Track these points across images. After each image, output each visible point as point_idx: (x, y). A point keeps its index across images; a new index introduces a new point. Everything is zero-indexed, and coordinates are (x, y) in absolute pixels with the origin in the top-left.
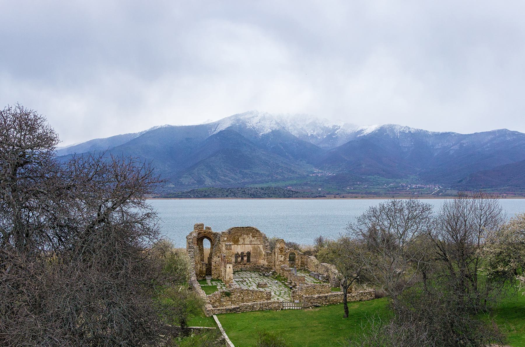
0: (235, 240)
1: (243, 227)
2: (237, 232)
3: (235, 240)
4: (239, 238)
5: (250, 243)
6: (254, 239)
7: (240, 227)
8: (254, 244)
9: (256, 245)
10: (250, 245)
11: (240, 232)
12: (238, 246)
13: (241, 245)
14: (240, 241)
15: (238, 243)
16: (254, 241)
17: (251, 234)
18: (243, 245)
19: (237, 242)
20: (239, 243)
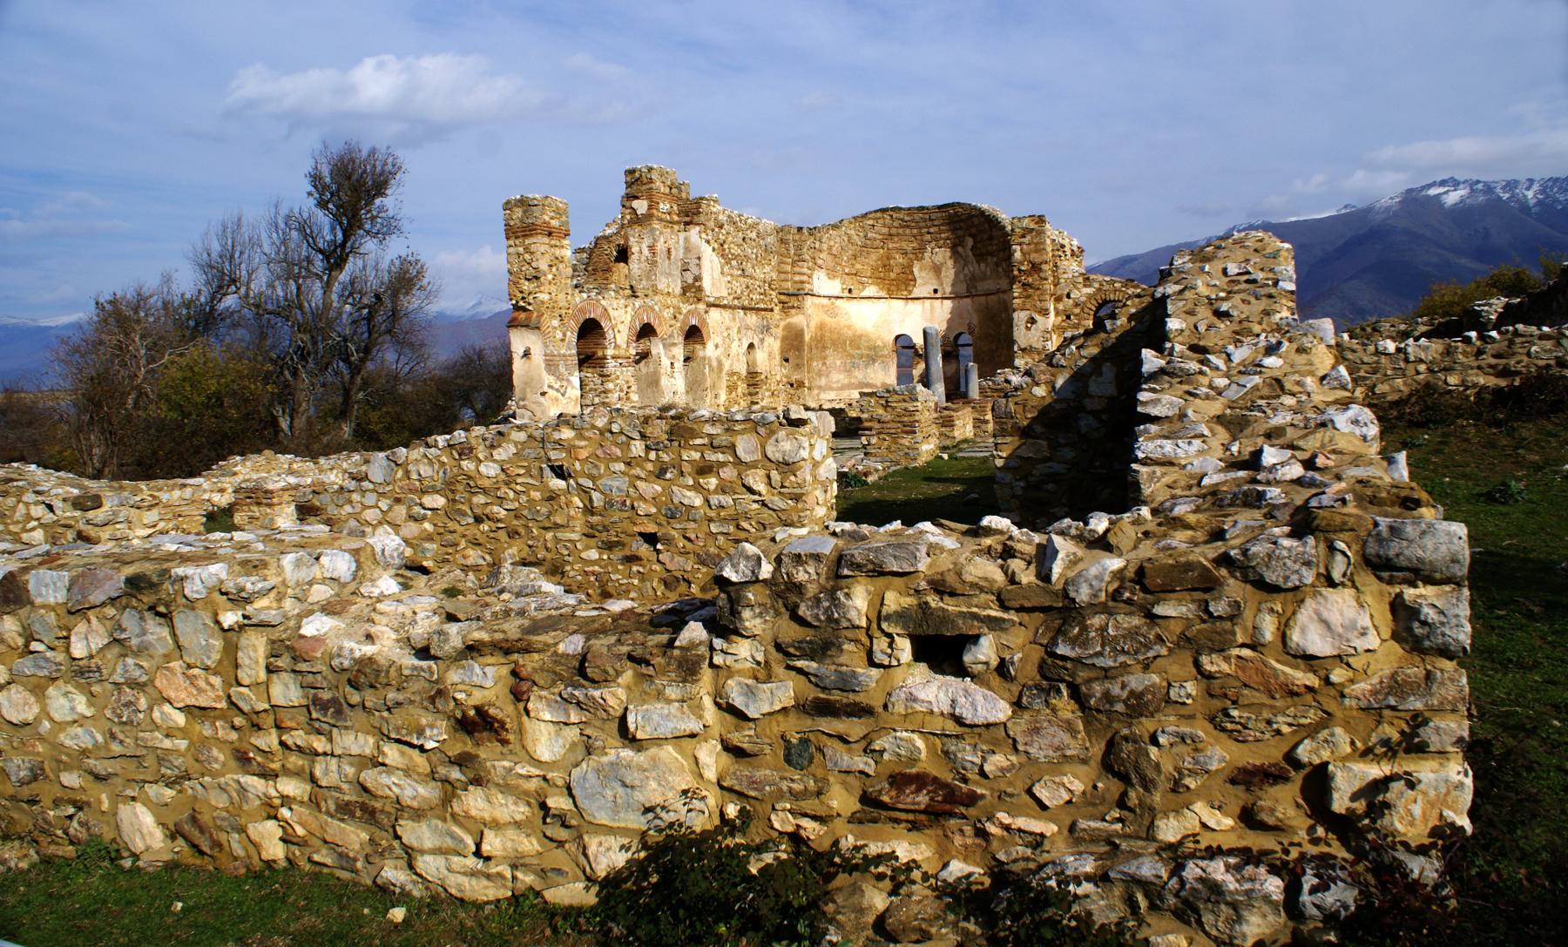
0: (893, 275)
1: (921, 209)
2: (894, 231)
3: (893, 275)
4: (910, 266)
5: (968, 291)
6: (983, 265)
7: (909, 209)
8: (987, 295)
9: (994, 298)
10: (968, 301)
11: (915, 231)
12: (912, 305)
13: (928, 302)
14: (919, 281)
15: (910, 292)
16: (984, 278)
17: (970, 242)
18: (939, 301)
19: (907, 285)
20: (917, 292)
